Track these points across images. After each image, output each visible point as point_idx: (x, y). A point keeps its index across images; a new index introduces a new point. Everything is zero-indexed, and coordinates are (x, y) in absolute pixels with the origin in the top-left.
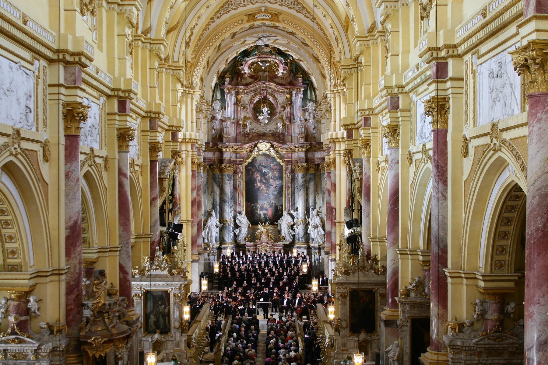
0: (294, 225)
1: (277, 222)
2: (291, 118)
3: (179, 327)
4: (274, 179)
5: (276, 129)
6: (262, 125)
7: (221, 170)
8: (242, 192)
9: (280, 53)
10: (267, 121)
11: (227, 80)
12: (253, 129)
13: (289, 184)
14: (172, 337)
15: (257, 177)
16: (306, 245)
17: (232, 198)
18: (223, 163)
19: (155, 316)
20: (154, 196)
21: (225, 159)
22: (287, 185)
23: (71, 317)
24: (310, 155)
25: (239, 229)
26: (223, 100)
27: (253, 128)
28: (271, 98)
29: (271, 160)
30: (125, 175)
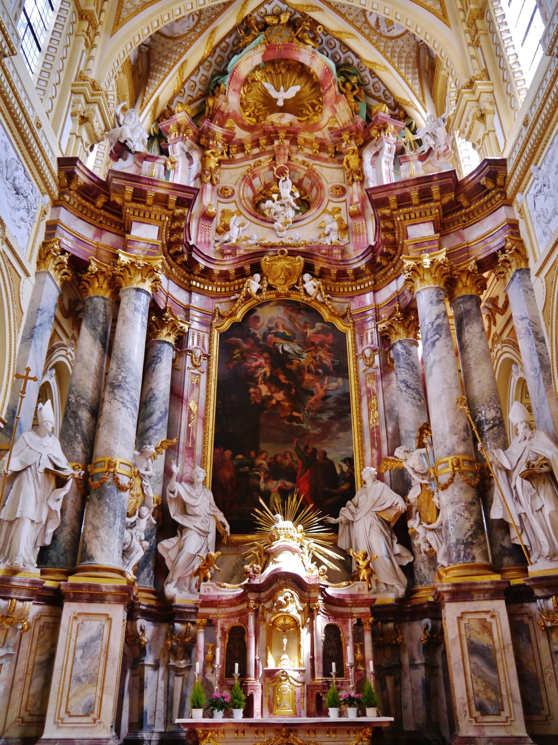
0: (405, 516)
1: (336, 516)
4: (317, 373)
5: (320, 237)
6: (276, 225)
8: (202, 413)
10: (291, 214)
13: (372, 385)
15: (260, 366)
16: (497, 577)
17: (160, 419)
22: (364, 389)
24: (452, 241)
25: (174, 540)
27: (248, 236)
29: (307, 319)
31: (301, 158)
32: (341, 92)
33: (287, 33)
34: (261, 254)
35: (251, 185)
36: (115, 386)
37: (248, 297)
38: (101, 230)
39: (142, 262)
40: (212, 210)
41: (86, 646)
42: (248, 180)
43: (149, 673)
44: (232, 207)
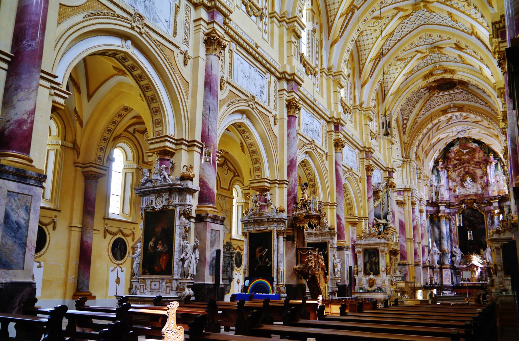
2: (487, 184)
3: (385, 271)
6: (467, 189)
7: (439, 218)
9: (475, 141)
11: (441, 163)
12: (461, 193)
13: (490, 227)
14: (380, 277)
15: (466, 223)
18: (440, 213)
19: (370, 264)
20: (370, 196)
21: (441, 210)
23: (290, 208)
26: (438, 176)
28: (472, 172)
30: (339, 165)
31: (471, 168)
32: (480, 148)
33: (464, 141)
34: (464, 200)
35: (460, 177)
36: (443, 238)
37: (462, 208)
38: (433, 207)
39: (443, 215)
40: (451, 188)
41: (447, 274)
42: (459, 176)
43: (453, 277)
44: (455, 184)
